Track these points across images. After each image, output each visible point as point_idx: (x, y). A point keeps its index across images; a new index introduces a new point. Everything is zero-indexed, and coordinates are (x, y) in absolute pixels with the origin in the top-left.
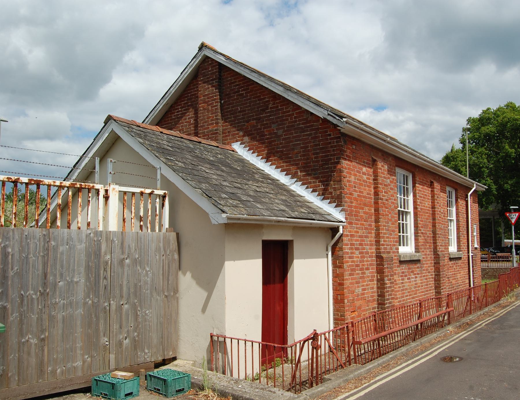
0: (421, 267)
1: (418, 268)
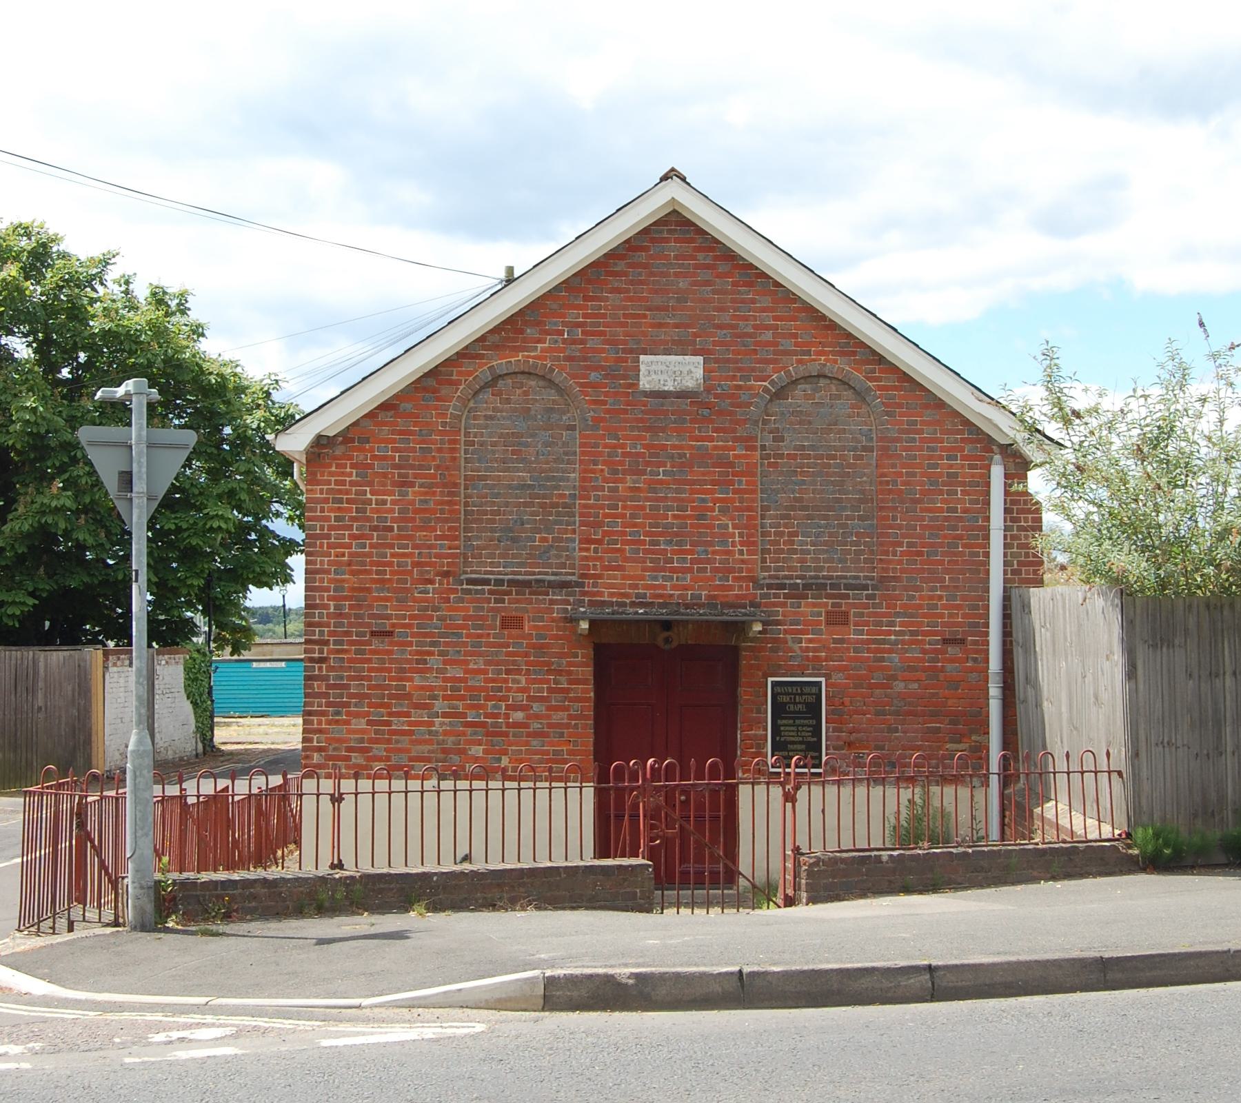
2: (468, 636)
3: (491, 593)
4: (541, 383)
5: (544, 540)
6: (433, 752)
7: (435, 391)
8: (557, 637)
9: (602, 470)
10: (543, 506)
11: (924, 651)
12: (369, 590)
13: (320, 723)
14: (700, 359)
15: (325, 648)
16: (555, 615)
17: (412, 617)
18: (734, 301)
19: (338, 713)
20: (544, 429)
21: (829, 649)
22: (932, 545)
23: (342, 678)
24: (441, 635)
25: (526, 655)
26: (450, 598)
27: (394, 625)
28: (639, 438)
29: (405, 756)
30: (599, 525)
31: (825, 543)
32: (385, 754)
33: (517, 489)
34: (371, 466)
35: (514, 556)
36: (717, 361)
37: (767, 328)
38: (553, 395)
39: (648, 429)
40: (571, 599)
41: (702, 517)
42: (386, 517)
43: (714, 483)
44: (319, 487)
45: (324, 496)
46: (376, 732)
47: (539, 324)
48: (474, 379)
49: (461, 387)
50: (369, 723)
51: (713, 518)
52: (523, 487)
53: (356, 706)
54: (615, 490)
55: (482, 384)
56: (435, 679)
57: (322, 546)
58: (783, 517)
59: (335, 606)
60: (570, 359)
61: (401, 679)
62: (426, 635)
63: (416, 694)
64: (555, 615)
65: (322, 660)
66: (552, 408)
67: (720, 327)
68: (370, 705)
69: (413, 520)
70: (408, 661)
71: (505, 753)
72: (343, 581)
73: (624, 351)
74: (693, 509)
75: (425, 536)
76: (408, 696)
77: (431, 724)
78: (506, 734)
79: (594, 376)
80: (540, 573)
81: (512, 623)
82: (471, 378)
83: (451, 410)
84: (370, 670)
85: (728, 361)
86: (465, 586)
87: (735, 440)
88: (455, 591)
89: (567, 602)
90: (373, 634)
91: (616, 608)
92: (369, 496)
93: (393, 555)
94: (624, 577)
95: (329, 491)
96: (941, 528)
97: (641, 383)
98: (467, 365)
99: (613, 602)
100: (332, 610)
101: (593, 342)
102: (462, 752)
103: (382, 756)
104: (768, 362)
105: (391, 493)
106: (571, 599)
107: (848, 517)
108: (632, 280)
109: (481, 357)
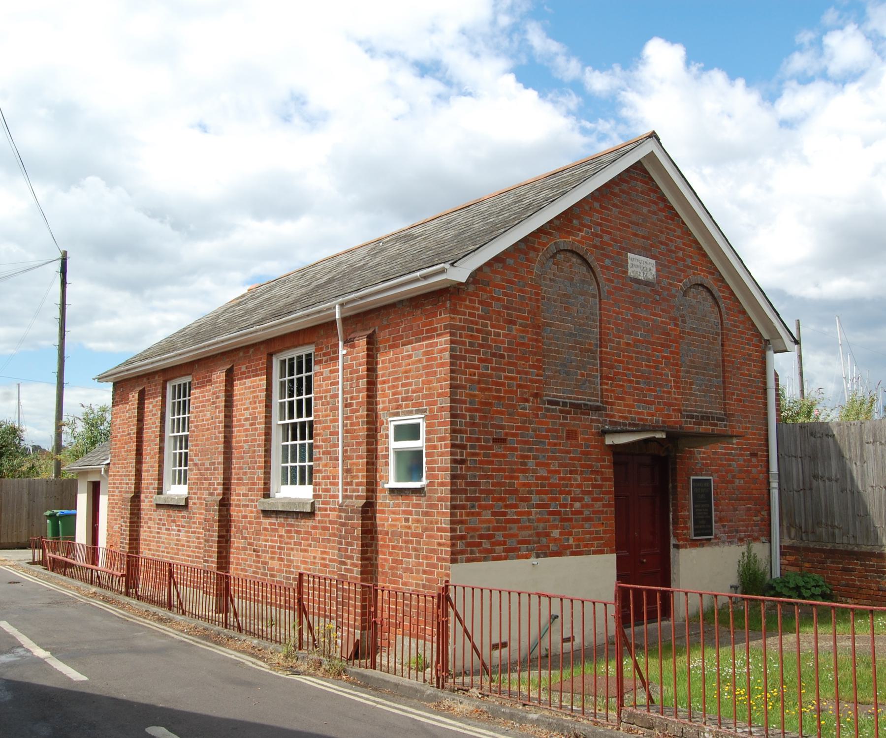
0: (191, 518)
1: (183, 517)
2: (550, 444)
3: (561, 411)
4: (579, 261)
5: (582, 375)
6: (530, 536)
7: (526, 254)
8: (595, 447)
9: (613, 328)
10: (581, 350)
11: (745, 461)
12: (490, 404)
13: (461, 515)
14: (653, 262)
15: (464, 451)
16: (593, 430)
17: (518, 428)
18: (666, 228)
19: (473, 507)
20: (581, 295)
21: (711, 458)
22: (745, 396)
23: (475, 477)
24: (534, 443)
25: (580, 459)
26: (538, 414)
27: (506, 434)
28: (629, 309)
29: (514, 540)
30: (611, 367)
31: (703, 391)
32: (503, 539)
33: (568, 336)
34: (490, 305)
35: (568, 386)
36: (661, 265)
37: (680, 249)
38: (584, 269)
39: (633, 303)
40: (601, 419)
41: (656, 367)
42: (500, 347)
43: (662, 345)
44: (458, 316)
45: (462, 324)
46: (498, 521)
47: (578, 218)
48: (547, 250)
49: (541, 254)
50: (494, 514)
51: (663, 369)
52: (571, 334)
53: (484, 500)
54: (618, 343)
55: (552, 254)
56: (531, 478)
57: (460, 366)
58: (688, 372)
59: (470, 416)
60: (595, 247)
61: (512, 478)
62: (526, 443)
63: (521, 489)
64: (593, 430)
65: (462, 462)
66: (584, 280)
67: (661, 243)
68: (494, 499)
69: (515, 351)
70: (516, 463)
71: (570, 534)
72: (475, 396)
73: (621, 248)
74: (654, 361)
75: (523, 364)
76: (516, 492)
77: (530, 513)
78: (570, 520)
79: (608, 262)
80: (581, 399)
81: (571, 435)
82: (545, 248)
83: (535, 270)
84: (493, 470)
85: (665, 266)
86: (546, 406)
87: (671, 318)
88: (540, 409)
89: (598, 421)
90: (495, 440)
91: (622, 427)
92: (489, 328)
93: (506, 378)
94: (625, 406)
95: (465, 321)
96: (746, 386)
97: (629, 272)
98: (544, 239)
99: (620, 422)
100: (468, 420)
101: (606, 238)
102: (547, 535)
103: (501, 541)
104: (680, 270)
105: (503, 328)
106: (601, 419)
107: (711, 376)
108: (622, 202)
109: (550, 234)
